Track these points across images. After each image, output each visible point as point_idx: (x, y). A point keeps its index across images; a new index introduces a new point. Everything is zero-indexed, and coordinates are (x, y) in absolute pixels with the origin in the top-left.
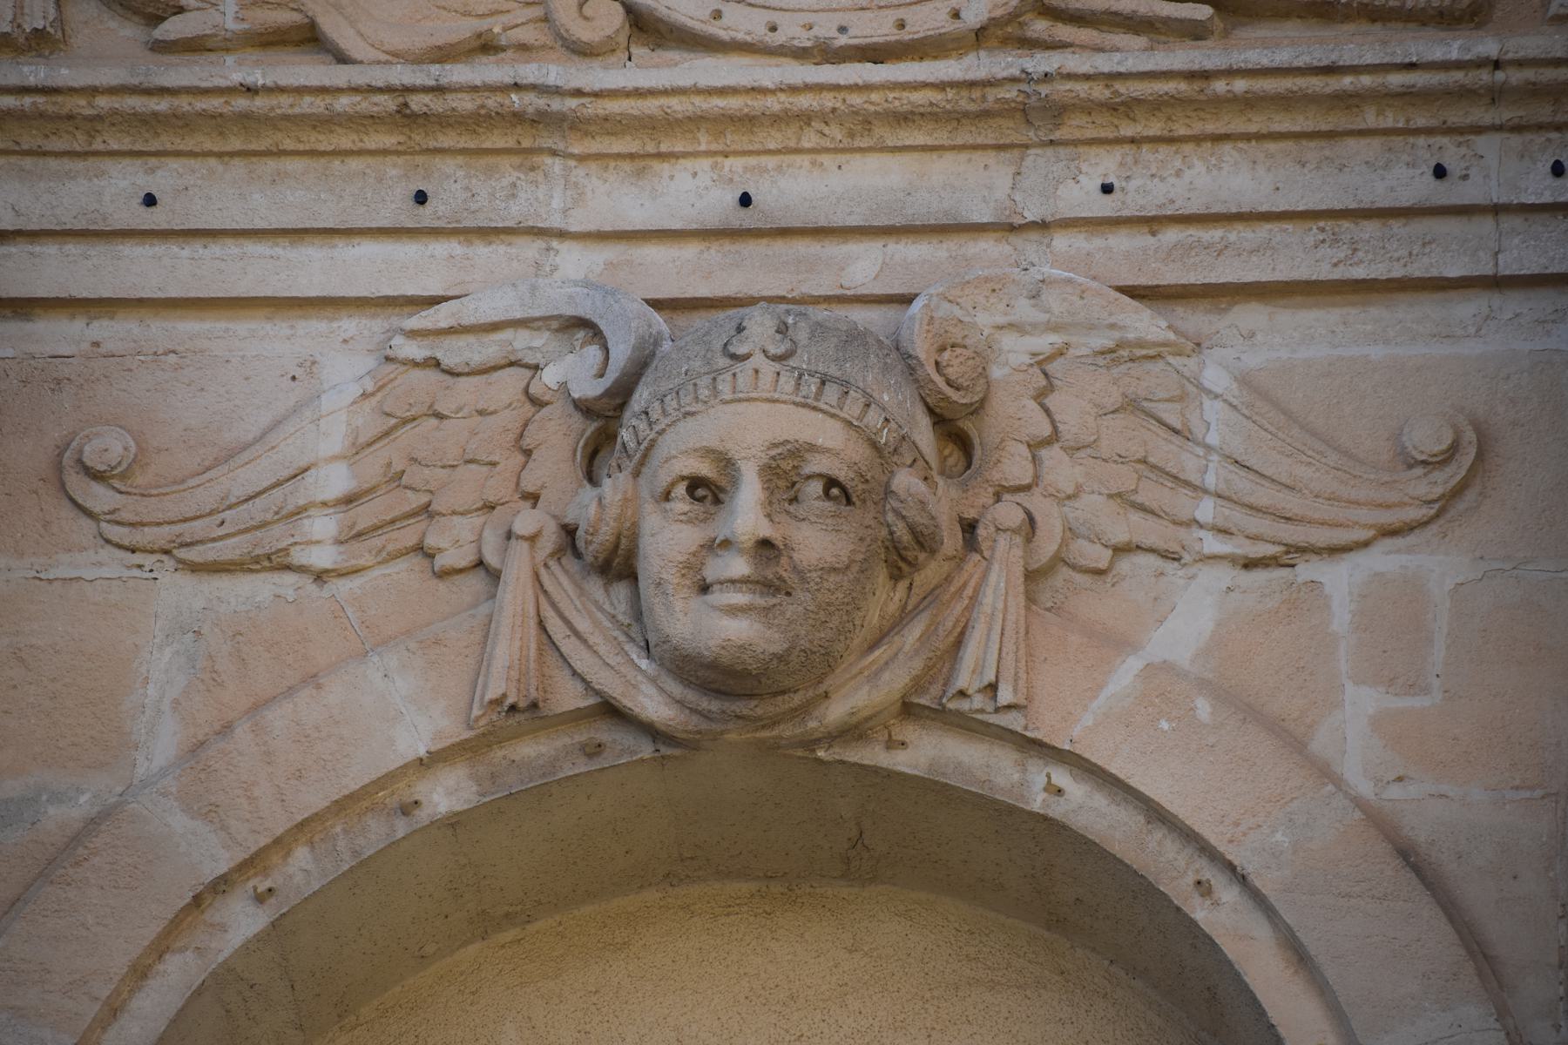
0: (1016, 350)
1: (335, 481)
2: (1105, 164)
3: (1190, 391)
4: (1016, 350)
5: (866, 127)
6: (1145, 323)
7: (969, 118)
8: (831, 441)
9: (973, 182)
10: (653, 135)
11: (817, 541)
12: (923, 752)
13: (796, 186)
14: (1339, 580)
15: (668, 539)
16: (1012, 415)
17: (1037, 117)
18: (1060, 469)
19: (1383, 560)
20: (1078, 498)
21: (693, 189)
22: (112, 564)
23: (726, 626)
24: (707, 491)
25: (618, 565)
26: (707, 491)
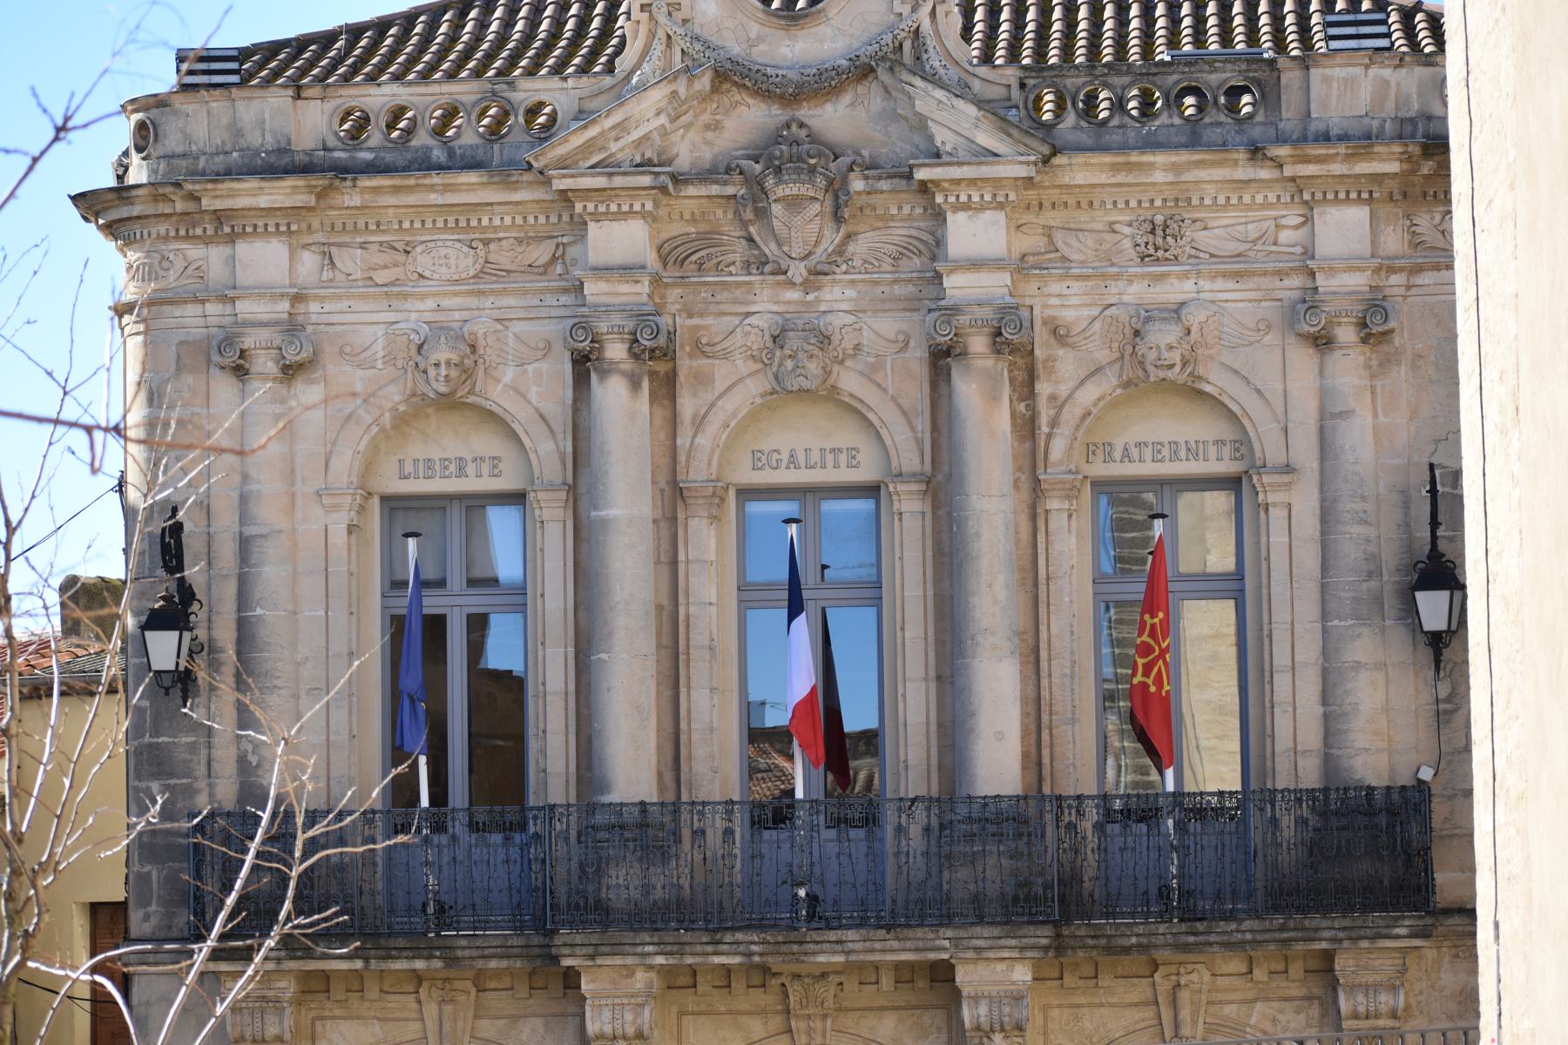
0: (481, 332)
1: (381, 354)
2: (491, 299)
3: (506, 337)
4: (481, 332)
5: (455, 294)
6: (500, 327)
7: (470, 293)
8: (454, 357)
9: (473, 302)
10: (424, 297)
11: (454, 373)
12: (471, 399)
13: (446, 303)
14: (530, 368)
15: (432, 372)
16: (481, 343)
17: (481, 293)
18: (489, 351)
19: (536, 365)
20: (491, 355)
21: (430, 304)
22: (348, 368)
23: (443, 389)
24: (437, 365)
25: (425, 372)
26: (437, 365)
